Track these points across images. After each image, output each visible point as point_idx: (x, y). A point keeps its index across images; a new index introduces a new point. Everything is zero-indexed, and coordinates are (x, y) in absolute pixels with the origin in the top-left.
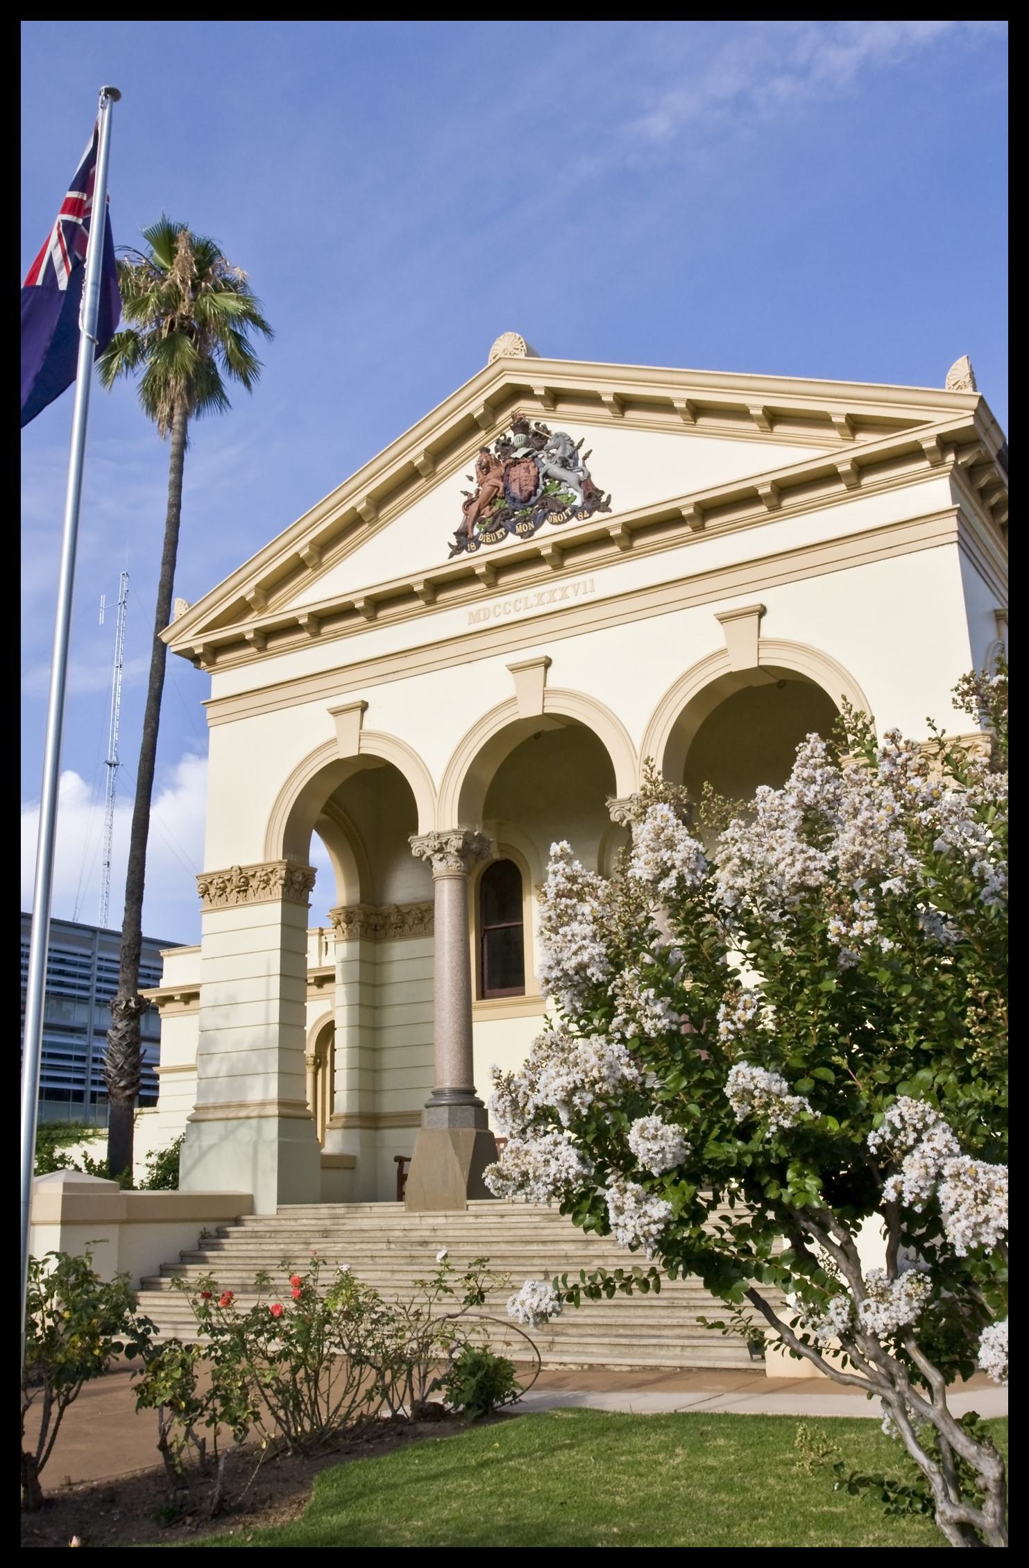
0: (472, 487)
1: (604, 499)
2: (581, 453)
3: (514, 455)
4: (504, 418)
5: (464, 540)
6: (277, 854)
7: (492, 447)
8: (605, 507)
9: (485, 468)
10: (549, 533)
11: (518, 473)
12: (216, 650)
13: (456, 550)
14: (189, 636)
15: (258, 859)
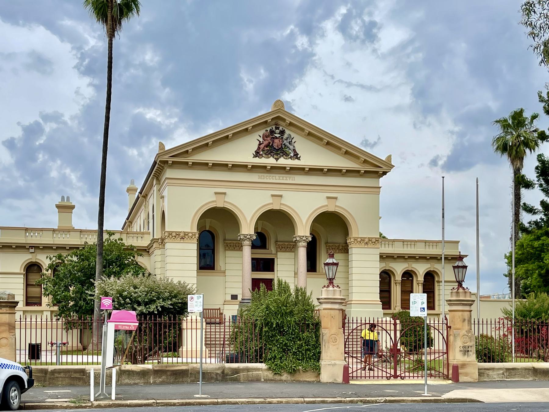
0: (261, 140)
1: (299, 156)
2: (293, 141)
3: (276, 135)
4: (274, 122)
5: (257, 154)
6: (195, 230)
7: (269, 129)
8: (299, 159)
9: (265, 137)
10: (283, 161)
11: (276, 141)
12: (174, 162)
13: (255, 156)
14: (167, 157)
15: (189, 230)
